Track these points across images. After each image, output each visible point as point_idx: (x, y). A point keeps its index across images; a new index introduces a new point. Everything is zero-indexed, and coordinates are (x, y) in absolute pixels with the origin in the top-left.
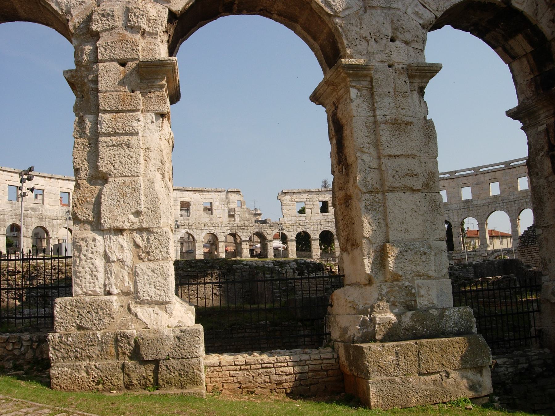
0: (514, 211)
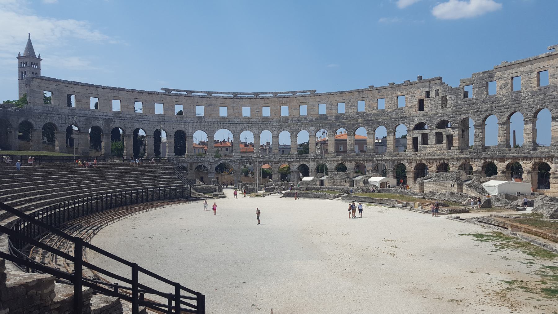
0: (238, 131)
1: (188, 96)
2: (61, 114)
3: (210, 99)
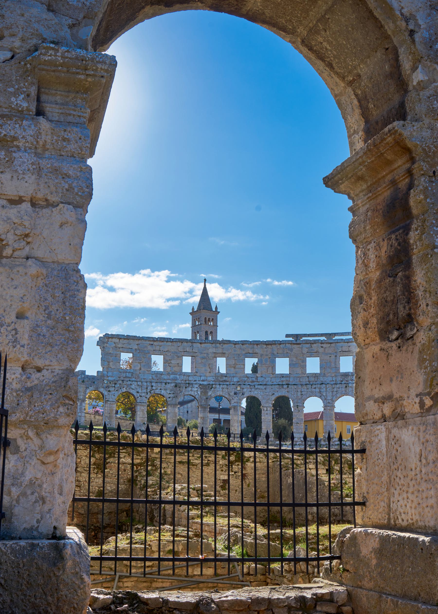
2: (143, 380)
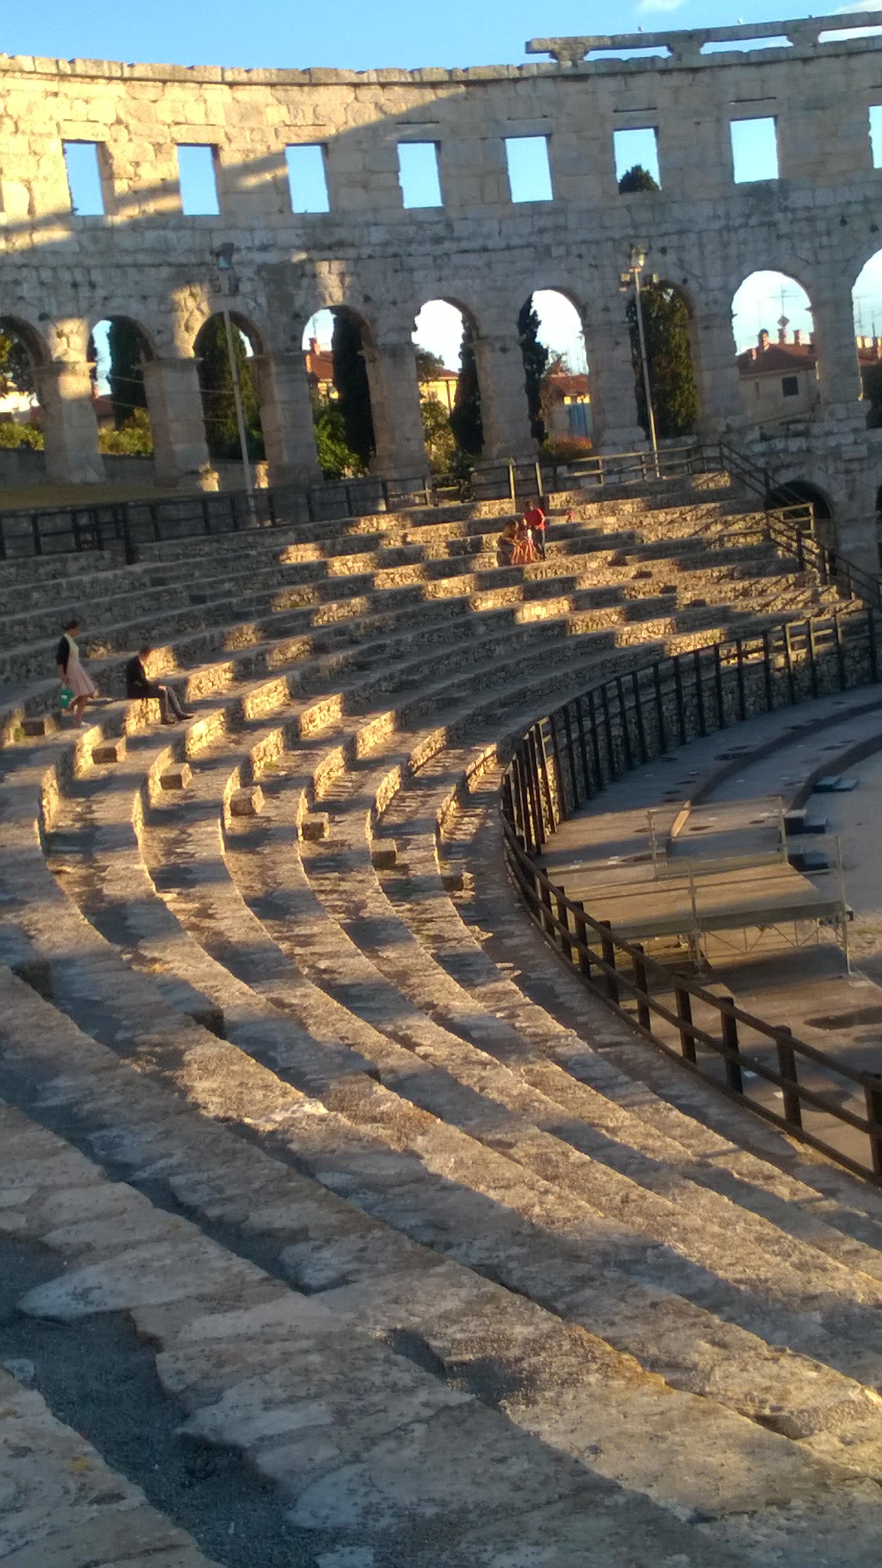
1: (680, 70)
3: (811, 69)
